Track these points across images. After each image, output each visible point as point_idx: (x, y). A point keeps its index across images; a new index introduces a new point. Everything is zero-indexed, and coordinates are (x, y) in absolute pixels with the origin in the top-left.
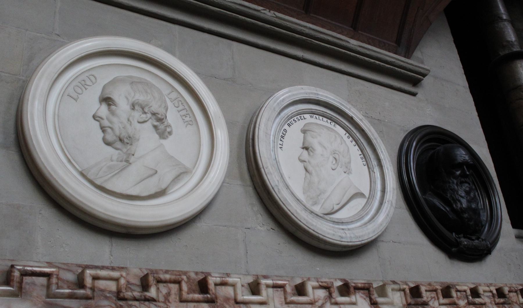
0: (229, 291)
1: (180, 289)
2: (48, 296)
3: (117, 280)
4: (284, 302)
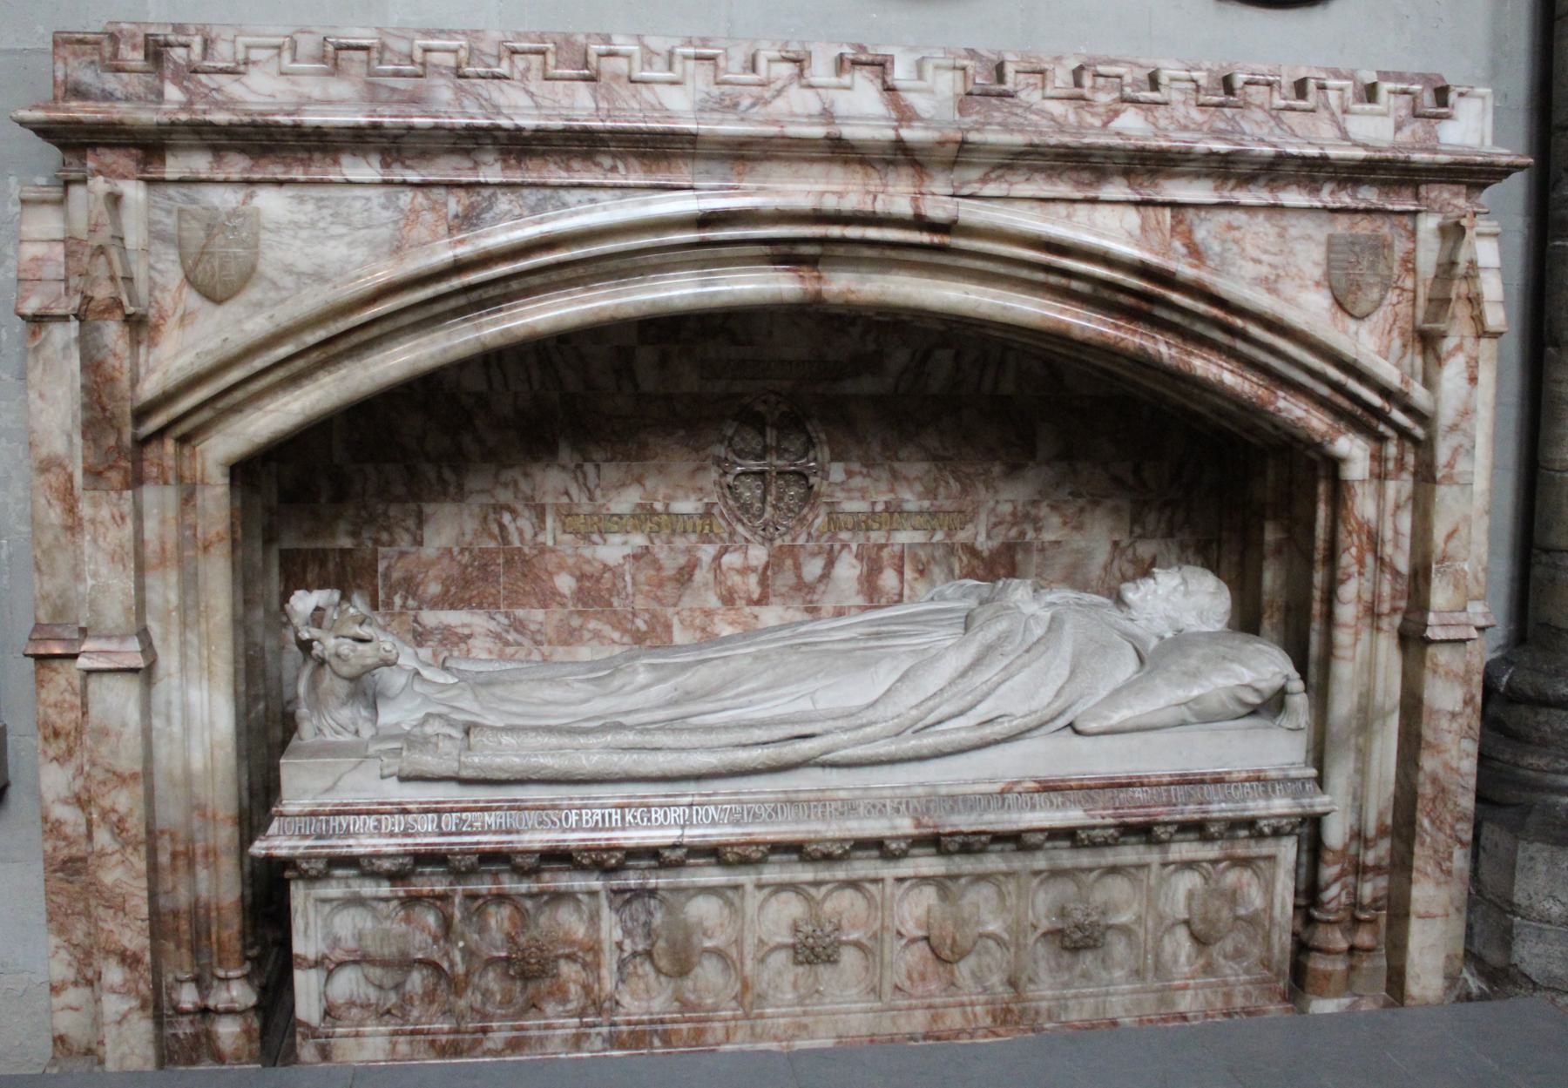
0: (620, 65)
1: (545, 63)
2: (369, 75)
3: (455, 51)
4: (712, 82)
